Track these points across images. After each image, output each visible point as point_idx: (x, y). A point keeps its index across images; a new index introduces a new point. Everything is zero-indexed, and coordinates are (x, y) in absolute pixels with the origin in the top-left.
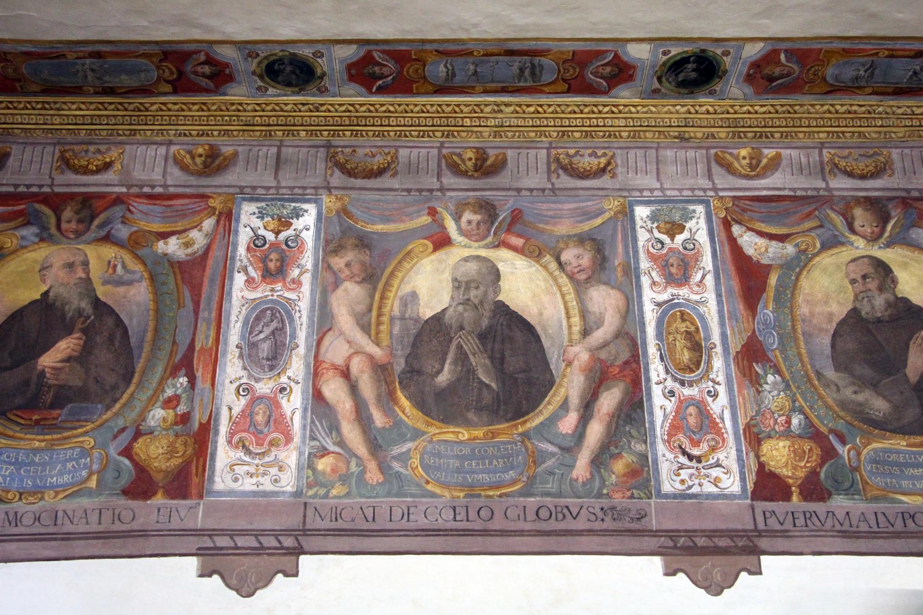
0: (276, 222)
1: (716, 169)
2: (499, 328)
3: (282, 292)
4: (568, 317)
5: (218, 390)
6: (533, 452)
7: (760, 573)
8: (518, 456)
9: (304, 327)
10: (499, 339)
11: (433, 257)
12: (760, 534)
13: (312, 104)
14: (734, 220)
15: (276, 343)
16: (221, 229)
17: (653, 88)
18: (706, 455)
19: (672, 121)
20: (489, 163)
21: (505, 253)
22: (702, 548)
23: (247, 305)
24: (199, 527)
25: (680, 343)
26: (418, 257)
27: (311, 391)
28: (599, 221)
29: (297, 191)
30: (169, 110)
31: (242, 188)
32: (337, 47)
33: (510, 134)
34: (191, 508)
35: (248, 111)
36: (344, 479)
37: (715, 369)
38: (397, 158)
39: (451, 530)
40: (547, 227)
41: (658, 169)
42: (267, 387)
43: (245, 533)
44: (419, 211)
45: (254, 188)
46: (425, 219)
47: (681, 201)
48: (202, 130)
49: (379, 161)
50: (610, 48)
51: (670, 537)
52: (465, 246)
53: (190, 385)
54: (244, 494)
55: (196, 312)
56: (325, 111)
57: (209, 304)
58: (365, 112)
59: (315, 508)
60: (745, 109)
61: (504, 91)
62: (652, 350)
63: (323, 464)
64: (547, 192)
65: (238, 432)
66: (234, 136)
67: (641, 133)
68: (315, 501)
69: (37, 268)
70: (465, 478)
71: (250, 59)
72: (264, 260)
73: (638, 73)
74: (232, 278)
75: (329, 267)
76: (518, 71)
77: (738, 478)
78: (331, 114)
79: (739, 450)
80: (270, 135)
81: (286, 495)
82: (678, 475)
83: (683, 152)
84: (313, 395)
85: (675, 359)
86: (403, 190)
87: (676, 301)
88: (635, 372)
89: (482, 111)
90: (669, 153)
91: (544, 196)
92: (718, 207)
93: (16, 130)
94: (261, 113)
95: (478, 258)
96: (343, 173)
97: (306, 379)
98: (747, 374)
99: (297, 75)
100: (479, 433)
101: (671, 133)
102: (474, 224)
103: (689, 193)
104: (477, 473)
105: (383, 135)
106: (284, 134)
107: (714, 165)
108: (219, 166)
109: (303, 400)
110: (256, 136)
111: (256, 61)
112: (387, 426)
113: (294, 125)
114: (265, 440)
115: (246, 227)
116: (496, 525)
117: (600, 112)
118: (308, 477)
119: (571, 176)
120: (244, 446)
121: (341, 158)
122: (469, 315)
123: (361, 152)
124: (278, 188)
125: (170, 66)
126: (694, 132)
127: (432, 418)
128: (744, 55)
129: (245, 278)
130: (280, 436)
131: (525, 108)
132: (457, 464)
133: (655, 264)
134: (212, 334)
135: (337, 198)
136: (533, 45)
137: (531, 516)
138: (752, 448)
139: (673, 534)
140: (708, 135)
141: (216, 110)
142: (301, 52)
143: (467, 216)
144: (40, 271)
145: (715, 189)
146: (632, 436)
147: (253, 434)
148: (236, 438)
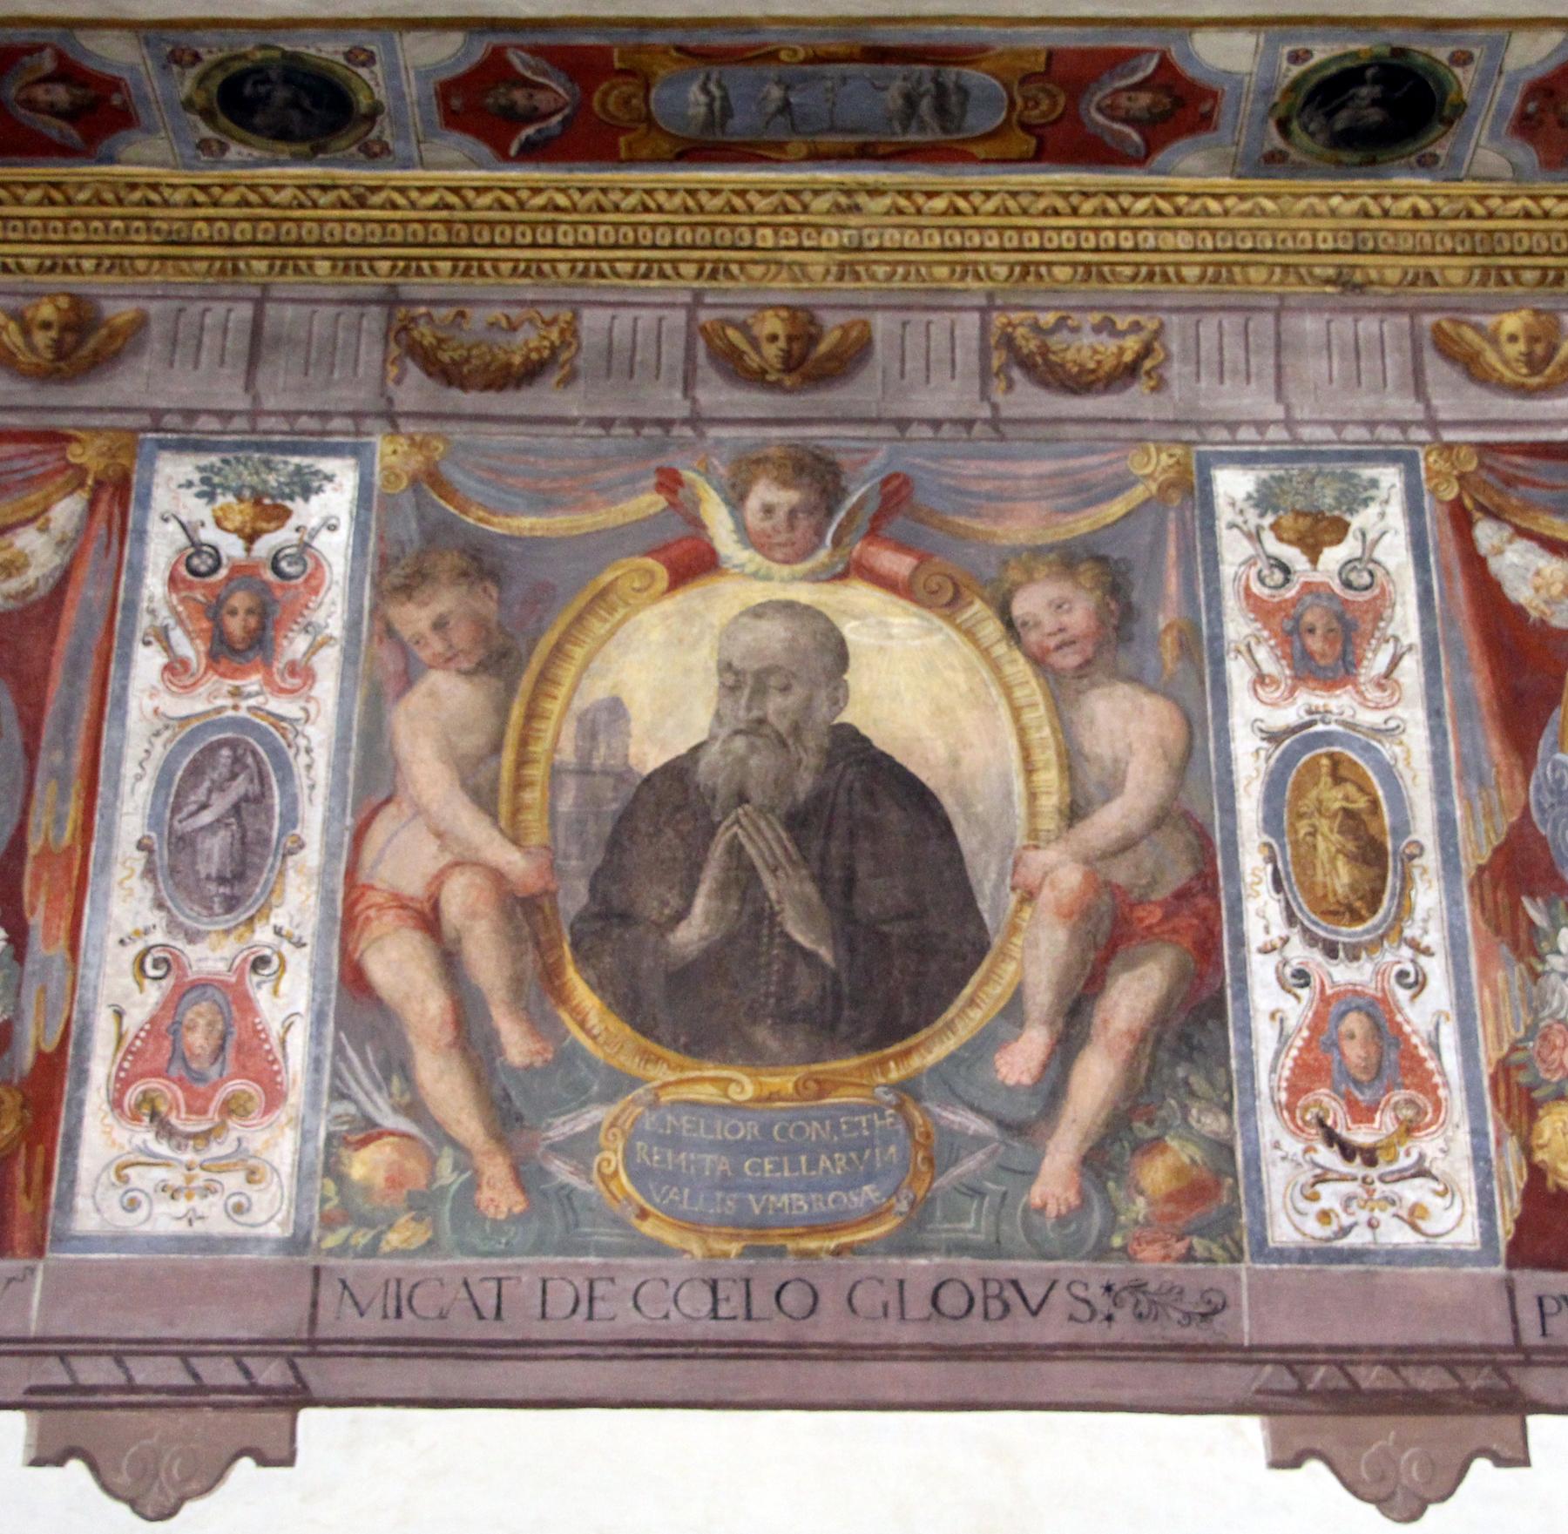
0: (247, 507)
1: (1437, 369)
2: (842, 798)
3: (261, 699)
4: (1029, 769)
5: (86, 964)
6: (928, 1135)
7: (1525, 1462)
8: (886, 1143)
9: (321, 792)
10: (840, 830)
11: (668, 605)
12: (1528, 1357)
13: (348, 188)
14: (1482, 508)
15: (243, 837)
16: (100, 527)
17: (1267, 148)
18: (1390, 1146)
19: (1320, 236)
20: (823, 347)
21: (861, 595)
22: (1375, 1393)
23: (167, 734)
24: (34, 1329)
25: (1329, 840)
26: (627, 604)
27: (335, 968)
28: (1116, 509)
29: (305, 422)
31: (157, 414)
32: (411, 38)
33: (881, 271)
34: (10, 1280)
35: (176, 205)
36: (422, 1204)
37: (1419, 914)
38: (575, 334)
39: (705, 1343)
40: (978, 525)
41: (1279, 367)
42: (218, 954)
43: (155, 1348)
44: (632, 480)
45: (191, 414)
46: (649, 502)
47: (1340, 456)
48: (53, 257)
49: (527, 341)
50: (1145, 44)
51: (1289, 1365)
52: (755, 575)
53: (11, 950)
54: (155, 1243)
55: (31, 752)
56: (382, 207)
57: (65, 729)
58: (490, 208)
59: (344, 1283)
60: (1516, 205)
61: (865, 154)
62: (1253, 862)
63: (364, 1165)
64: (978, 429)
65: (143, 1076)
66: (139, 273)
67: (1236, 270)
68: (342, 1262)
70: (742, 1203)
71: (175, 69)
72: (215, 610)
73: (1226, 105)
74: (126, 660)
75: (389, 631)
76: (900, 102)
77: (1472, 1207)
78: (398, 214)
79: (1478, 1133)
80: (236, 270)
81: (267, 1247)
82: (1314, 1198)
83: (1349, 319)
84: (342, 978)
85: (1313, 883)
86: (591, 422)
87: (1320, 727)
88: (1205, 919)
89: (805, 209)
90: (1311, 325)
91: (969, 440)
92: (1438, 473)
94: (211, 212)
95: (789, 608)
96: (430, 375)
97: (322, 936)
98: (1506, 927)
99: (305, 112)
100: (784, 1081)
101: (1317, 271)
102: (781, 515)
103: (1361, 433)
104: (779, 1190)
105: (540, 272)
106: (271, 267)
107: (1430, 357)
108: (96, 353)
109: (314, 988)
112: (538, 1062)
113: (300, 243)
114: (209, 1099)
115: (166, 520)
116: (826, 1328)
117: (1125, 212)
118: (324, 1200)
119: (1044, 384)
120: (154, 1115)
121: (425, 334)
122: (762, 764)
123: (479, 317)
124: (254, 414)
126: (1380, 268)
127: (658, 1040)
129: (161, 660)
130: (253, 1088)
131: (920, 200)
132: (724, 1164)
133: (1265, 626)
134: (73, 809)
135: (413, 443)
136: (939, 35)
137: (918, 1305)
138: (1512, 1126)
139: (1293, 1358)
140: (1417, 276)
141: (87, 203)
142: (312, 51)
143: (764, 493)
145: (1433, 424)
146: (1192, 1094)
147: (180, 1081)
148: (132, 1095)
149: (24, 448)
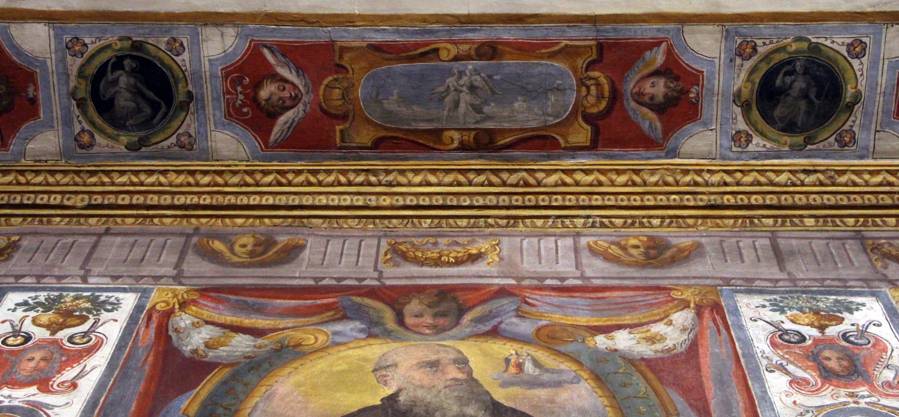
30: (577, 184)
35: (713, 185)
69: (370, 367)
71: (738, 61)
93: (313, 220)
99: (810, 102)
110: (726, 226)
111: (748, 64)
125: (603, 80)
142: (828, 43)
144: (375, 370)
149: (640, 293)
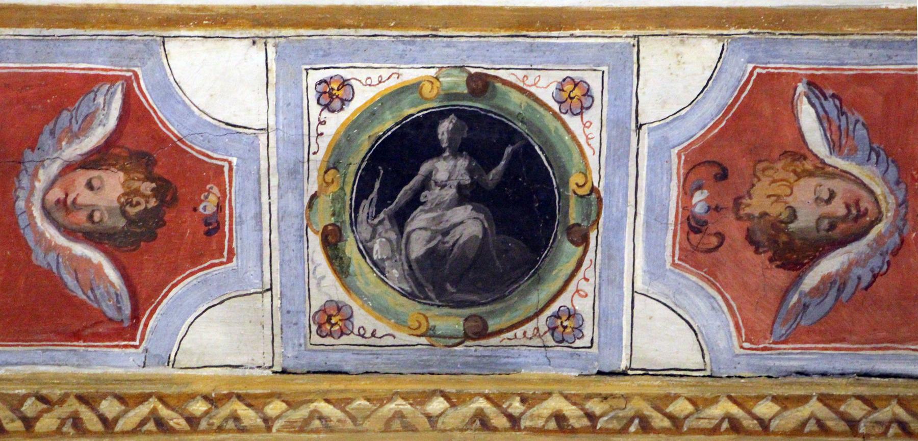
50: (99, 65)
128: (650, 113)
